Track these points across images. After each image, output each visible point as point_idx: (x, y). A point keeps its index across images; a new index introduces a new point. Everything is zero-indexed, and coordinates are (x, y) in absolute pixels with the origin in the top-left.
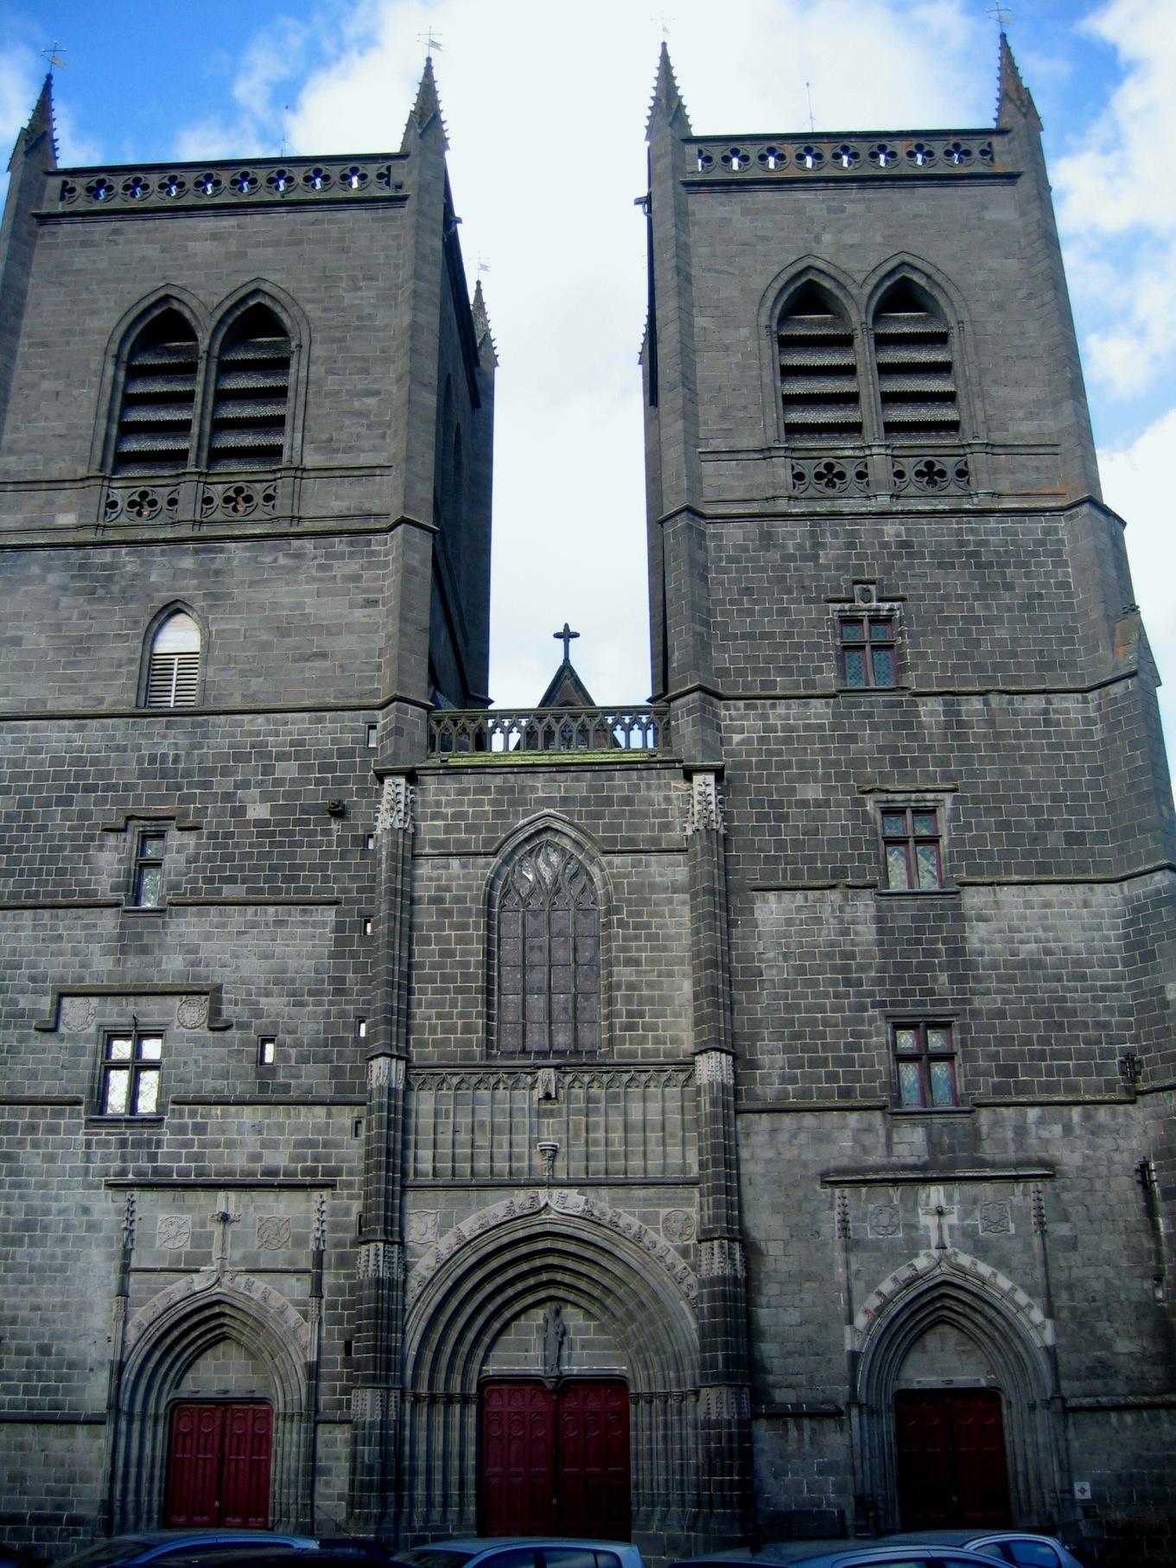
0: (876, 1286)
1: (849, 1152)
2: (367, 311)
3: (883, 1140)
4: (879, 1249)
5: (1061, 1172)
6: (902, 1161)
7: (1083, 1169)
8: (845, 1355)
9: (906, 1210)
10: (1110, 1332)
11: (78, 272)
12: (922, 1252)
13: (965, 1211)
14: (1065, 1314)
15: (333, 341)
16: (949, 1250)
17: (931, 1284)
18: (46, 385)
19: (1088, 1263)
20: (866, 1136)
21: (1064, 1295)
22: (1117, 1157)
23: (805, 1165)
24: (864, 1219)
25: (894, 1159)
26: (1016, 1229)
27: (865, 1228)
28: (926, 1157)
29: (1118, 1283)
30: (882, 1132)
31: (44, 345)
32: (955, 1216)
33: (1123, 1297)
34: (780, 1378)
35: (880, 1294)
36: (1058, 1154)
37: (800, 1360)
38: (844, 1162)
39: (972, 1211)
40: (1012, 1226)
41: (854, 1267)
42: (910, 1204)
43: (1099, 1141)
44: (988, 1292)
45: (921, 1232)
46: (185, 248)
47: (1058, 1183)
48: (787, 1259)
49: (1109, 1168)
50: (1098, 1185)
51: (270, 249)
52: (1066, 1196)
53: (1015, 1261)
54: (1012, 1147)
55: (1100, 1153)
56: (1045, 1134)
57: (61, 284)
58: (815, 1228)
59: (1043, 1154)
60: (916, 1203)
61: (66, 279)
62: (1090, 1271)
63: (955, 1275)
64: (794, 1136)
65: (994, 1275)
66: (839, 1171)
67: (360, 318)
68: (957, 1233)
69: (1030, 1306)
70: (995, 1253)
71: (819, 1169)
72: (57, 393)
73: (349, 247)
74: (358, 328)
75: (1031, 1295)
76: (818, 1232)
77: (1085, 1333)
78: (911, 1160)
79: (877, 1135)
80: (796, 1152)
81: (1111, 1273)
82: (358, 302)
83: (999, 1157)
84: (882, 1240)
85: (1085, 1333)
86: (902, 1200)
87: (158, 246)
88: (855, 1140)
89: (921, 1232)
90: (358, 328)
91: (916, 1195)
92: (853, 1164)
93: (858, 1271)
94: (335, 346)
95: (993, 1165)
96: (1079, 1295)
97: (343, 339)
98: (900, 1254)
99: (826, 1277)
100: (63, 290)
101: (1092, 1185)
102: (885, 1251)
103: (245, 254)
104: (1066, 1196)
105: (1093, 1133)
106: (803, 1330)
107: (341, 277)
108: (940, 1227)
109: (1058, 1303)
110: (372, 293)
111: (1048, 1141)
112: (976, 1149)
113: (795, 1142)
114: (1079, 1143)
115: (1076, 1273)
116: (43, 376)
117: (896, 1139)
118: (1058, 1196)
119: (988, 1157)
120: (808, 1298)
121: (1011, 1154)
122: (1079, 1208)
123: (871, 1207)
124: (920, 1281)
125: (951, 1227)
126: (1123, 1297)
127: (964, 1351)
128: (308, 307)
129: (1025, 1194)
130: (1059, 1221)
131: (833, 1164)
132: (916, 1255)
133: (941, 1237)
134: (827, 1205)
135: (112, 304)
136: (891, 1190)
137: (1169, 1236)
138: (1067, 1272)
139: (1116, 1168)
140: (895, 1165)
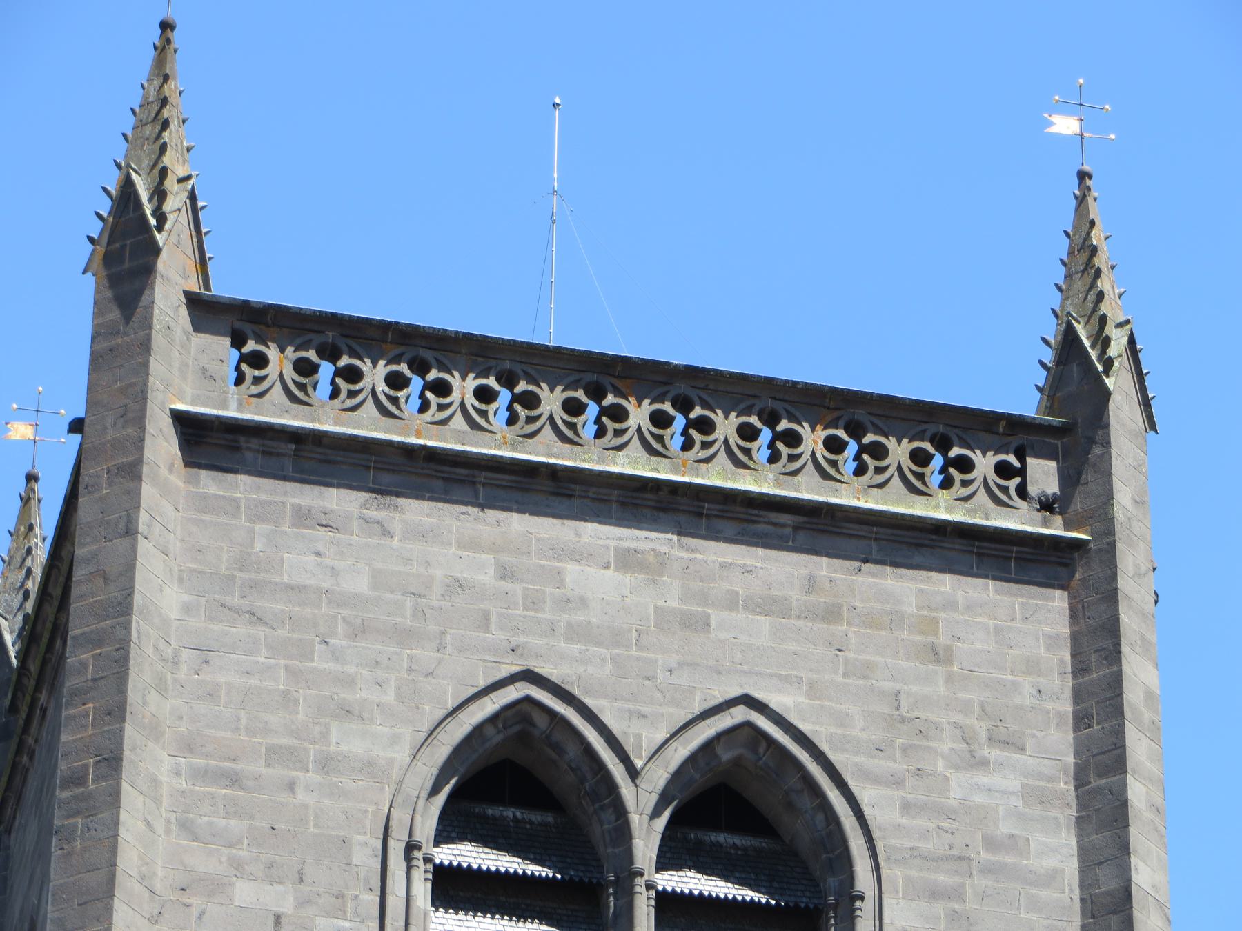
2: (1005, 828)
11: (295, 590)
15: (936, 894)
18: (245, 892)
31: (234, 780)
46: (558, 578)
51: (764, 622)
57: (256, 618)
61: (269, 605)
67: (991, 844)
72: (278, 919)
73: (948, 649)
74: (989, 870)
82: (979, 799)
87: (488, 558)
90: (989, 870)
94: (939, 908)
97: (955, 894)
100: (261, 632)
103: (704, 625)
107: (937, 727)
110: (1015, 783)
116: (238, 866)
128: (865, 795)
135: (390, 697)
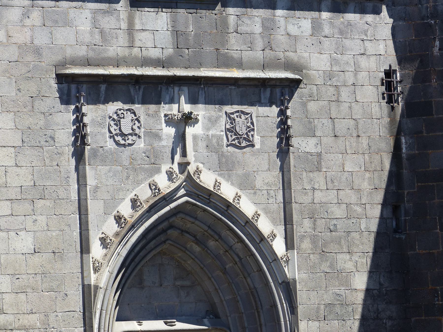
0: (116, 206)
1: (87, 39)
3: (124, 25)
4: (116, 161)
5: (308, 76)
6: (145, 53)
7: (330, 75)
10: (350, 266)
12: (165, 168)
13: (210, 119)
14: (306, 245)
16: (191, 168)
19: (330, 185)
20: (107, 19)
21: (307, 223)
22: (363, 62)
23: (37, 51)
25: (136, 51)
26: (262, 143)
28: (170, 51)
29: (359, 209)
30: (123, 15)
33: (363, 227)
34: (10, 318)
35: (119, 219)
37: (32, 296)
38: (82, 52)
40: (257, 140)
41: (91, 181)
43: (347, 43)
48: (18, 169)
49: (356, 75)
50: (345, 94)
52: (312, 106)
53: (259, 183)
54: (260, 44)
55: (347, 58)
56: (293, 30)
58: (49, 133)
59: (291, 54)
62: (332, 195)
64: (26, 15)
65: (237, 197)
66: (74, 62)
68: (202, 145)
70: (240, 172)
71: (58, 58)
75: (274, 222)
76: (53, 138)
77: (325, 267)
78: (155, 53)
79: (118, 20)
80: (29, 34)
81: (353, 199)
83: (247, 55)
85: (325, 267)
88: (95, 24)
92: (91, 54)
95: (240, 65)
96: (321, 223)
99: (62, 194)
101: (339, 94)
102: (126, 163)
104: (312, 106)
105: (341, 32)
106: (37, 259)
109: (298, 231)
111: (296, 38)
112: (224, 42)
113: (28, 22)
114: (326, 43)
115: (319, 196)
117: (138, 26)
119: (235, 55)
120: (42, 220)
121: (259, 55)
122: (325, 121)
125: (195, 137)
126: (363, 227)
127: (182, 287)
131: (69, 53)
132: (158, 171)
137: (411, 158)
138: (310, 194)
139: (363, 75)
140: (136, 57)
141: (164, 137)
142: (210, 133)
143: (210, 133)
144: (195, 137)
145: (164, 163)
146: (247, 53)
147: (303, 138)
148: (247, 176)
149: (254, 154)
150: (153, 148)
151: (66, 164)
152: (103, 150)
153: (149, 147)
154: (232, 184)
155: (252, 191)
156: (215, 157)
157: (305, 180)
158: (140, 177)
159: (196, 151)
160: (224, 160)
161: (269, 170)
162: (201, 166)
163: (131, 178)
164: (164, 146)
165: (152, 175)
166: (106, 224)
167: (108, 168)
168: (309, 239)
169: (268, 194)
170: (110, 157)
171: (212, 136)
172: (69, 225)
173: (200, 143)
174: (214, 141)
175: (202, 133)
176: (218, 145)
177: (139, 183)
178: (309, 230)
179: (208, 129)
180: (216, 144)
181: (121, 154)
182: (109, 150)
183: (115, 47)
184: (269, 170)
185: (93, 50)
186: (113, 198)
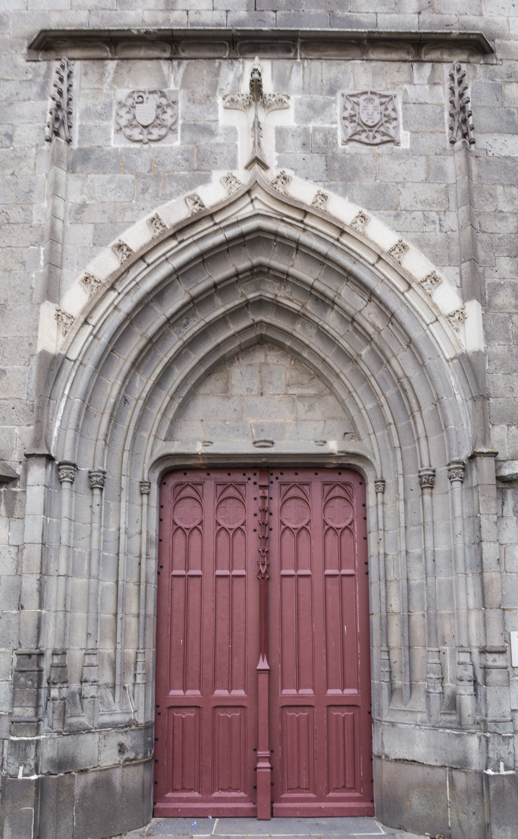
0: (115, 234)
8: (34, 363)
9: (192, 100)
12: (217, 175)
13: (311, 106)
17: (230, 233)
24: (103, 115)
27: (105, 131)
32: (291, 112)
36: (501, 20)
39: (327, 105)
42: (202, 90)
44: (347, 252)
45: (219, 139)
47: (501, 69)
60: (214, 87)
63: (282, 219)
69: (435, 279)
70: (369, 182)
75: (436, 260)
84: (139, 152)
86: (185, 85)
89: (219, 139)
91: (217, 74)
93: (82, 207)
98: (171, 177)
102: (143, 170)
108: (257, 126)
118: (498, 89)
123: (122, 94)
124: (206, 224)
125: (280, 133)
129: (433, 83)
130: (500, 132)
132: (205, 180)
133: (257, 144)
134: (35, 89)
136: (165, 66)
141: (220, 131)
142: (311, 125)
143: (311, 125)
144: (280, 133)
145: (218, 168)
146: (387, 16)
147: (496, 136)
148: (382, 189)
149: (396, 156)
150: (197, 147)
151: (30, 172)
152: (103, 151)
153: (191, 146)
154: (352, 200)
155: (393, 213)
156: (319, 161)
157: (501, 199)
158: (169, 190)
159: (279, 149)
160: (337, 165)
161: (426, 180)
162: (289, 173)
163: (150, 191)
164: (218, 144)
165: (191, 187)
166: (95, 261)
167: (108, 176)
168: (509, 291)
169: (426, 218)
170: (115, 160)
171: (315, 129)
172: (23, 263)
173: (290, 140)
174: (319, 137)
175: (295, 125)
176: (326, 142)
177: (166, 198)
178: (508, 275)
179: (308, 120)
180: (321, 142)
181: (135, 156)
182: (112, 151)
183: (140, 11)
184: (426, 180)
185: (97, 15)
186: (113, 222)
